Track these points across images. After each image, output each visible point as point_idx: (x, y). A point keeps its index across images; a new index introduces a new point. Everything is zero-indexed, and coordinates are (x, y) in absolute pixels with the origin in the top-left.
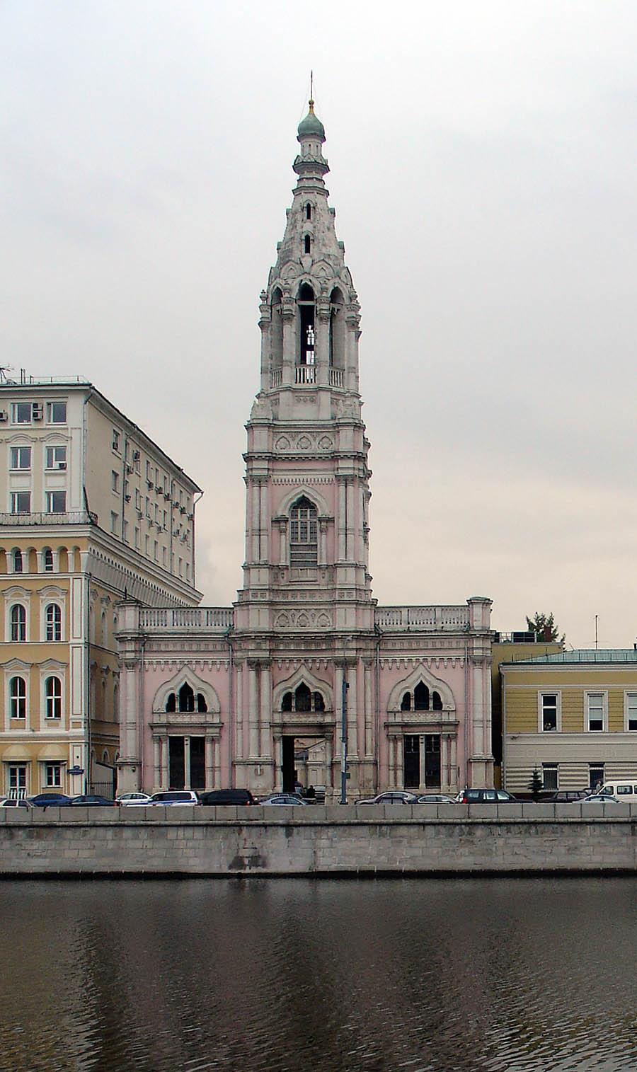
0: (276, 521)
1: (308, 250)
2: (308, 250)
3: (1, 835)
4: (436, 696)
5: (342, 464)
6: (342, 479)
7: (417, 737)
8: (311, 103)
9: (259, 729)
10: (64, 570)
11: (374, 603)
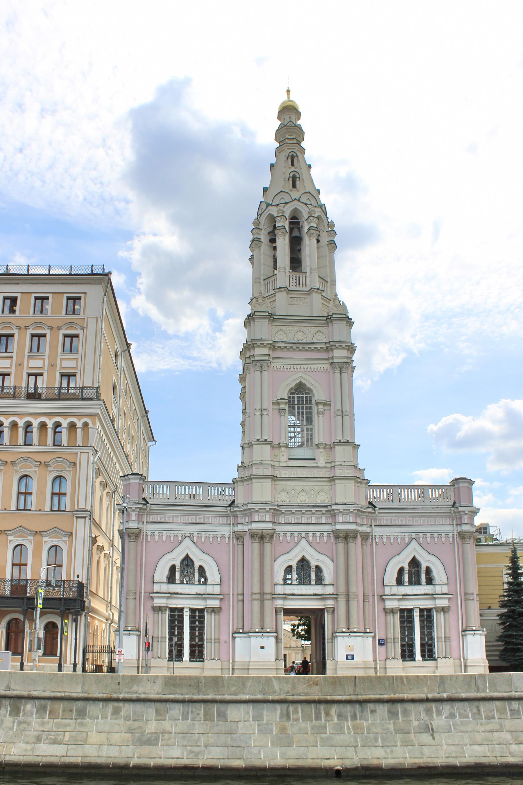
0: (277, 403)
1: (294, 186)
2: (294, 186)
3: (4, 712)
4: (428, 571)
5: (336, 353)
6: (338, 366)
7: (411, 611)
8: (288, 91)
9: (262, 601)
10: (72, 443)
11: (368, 482)
